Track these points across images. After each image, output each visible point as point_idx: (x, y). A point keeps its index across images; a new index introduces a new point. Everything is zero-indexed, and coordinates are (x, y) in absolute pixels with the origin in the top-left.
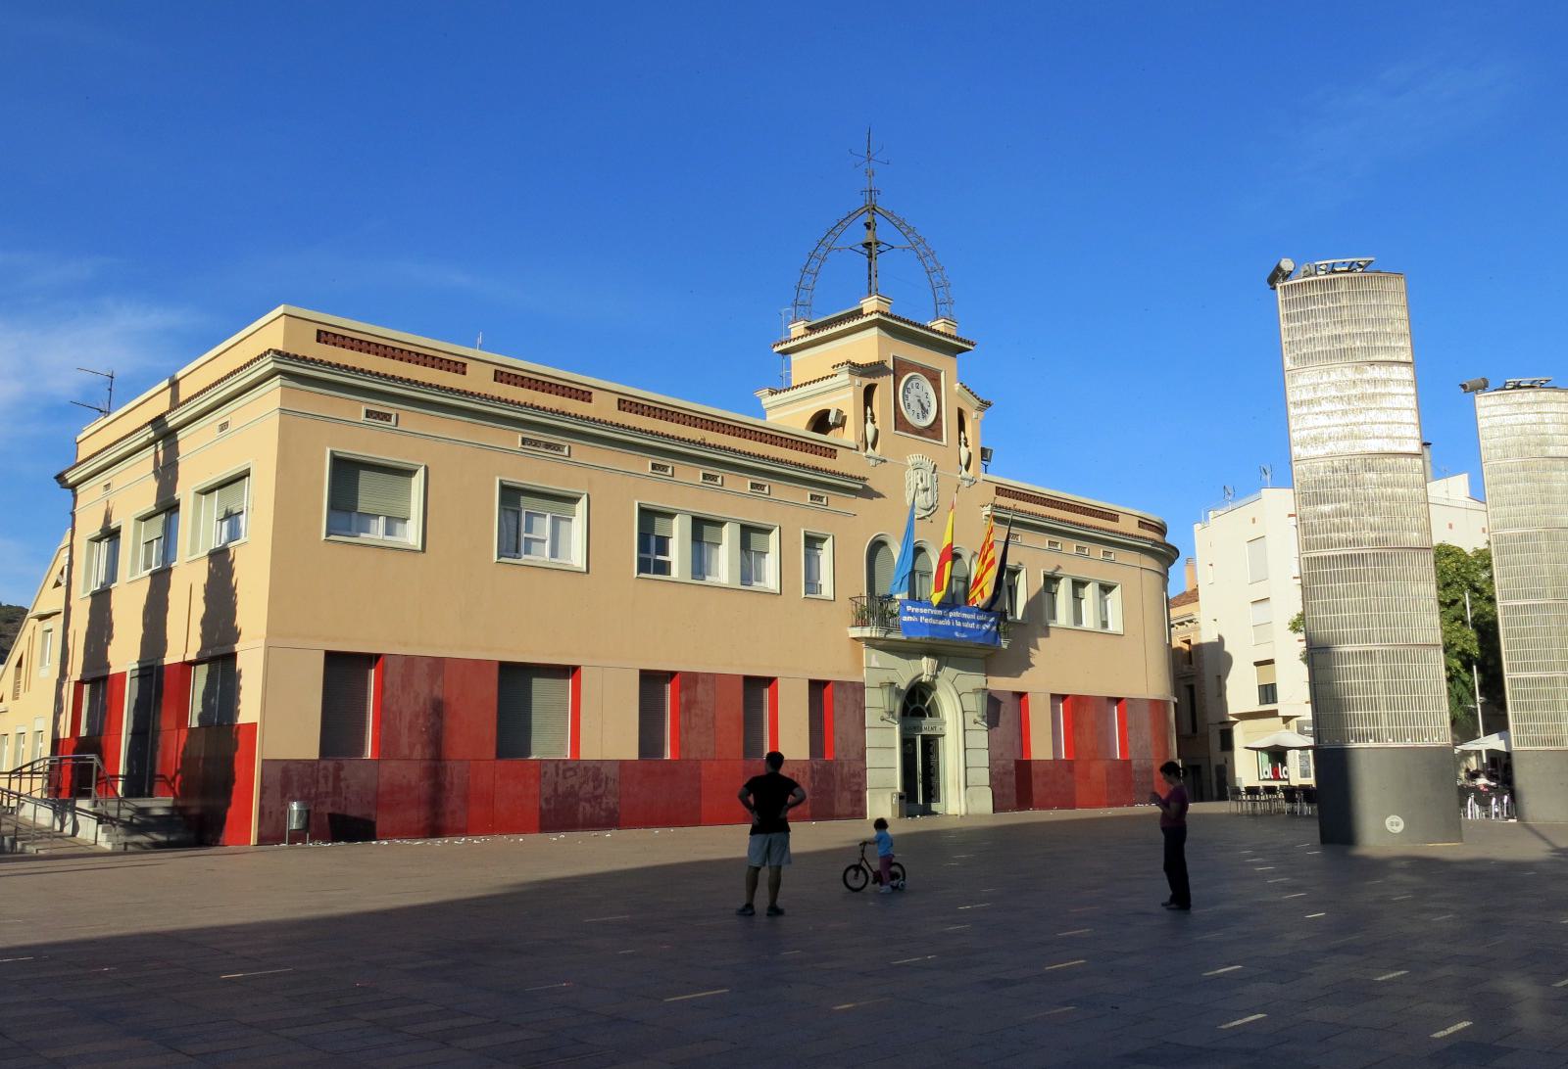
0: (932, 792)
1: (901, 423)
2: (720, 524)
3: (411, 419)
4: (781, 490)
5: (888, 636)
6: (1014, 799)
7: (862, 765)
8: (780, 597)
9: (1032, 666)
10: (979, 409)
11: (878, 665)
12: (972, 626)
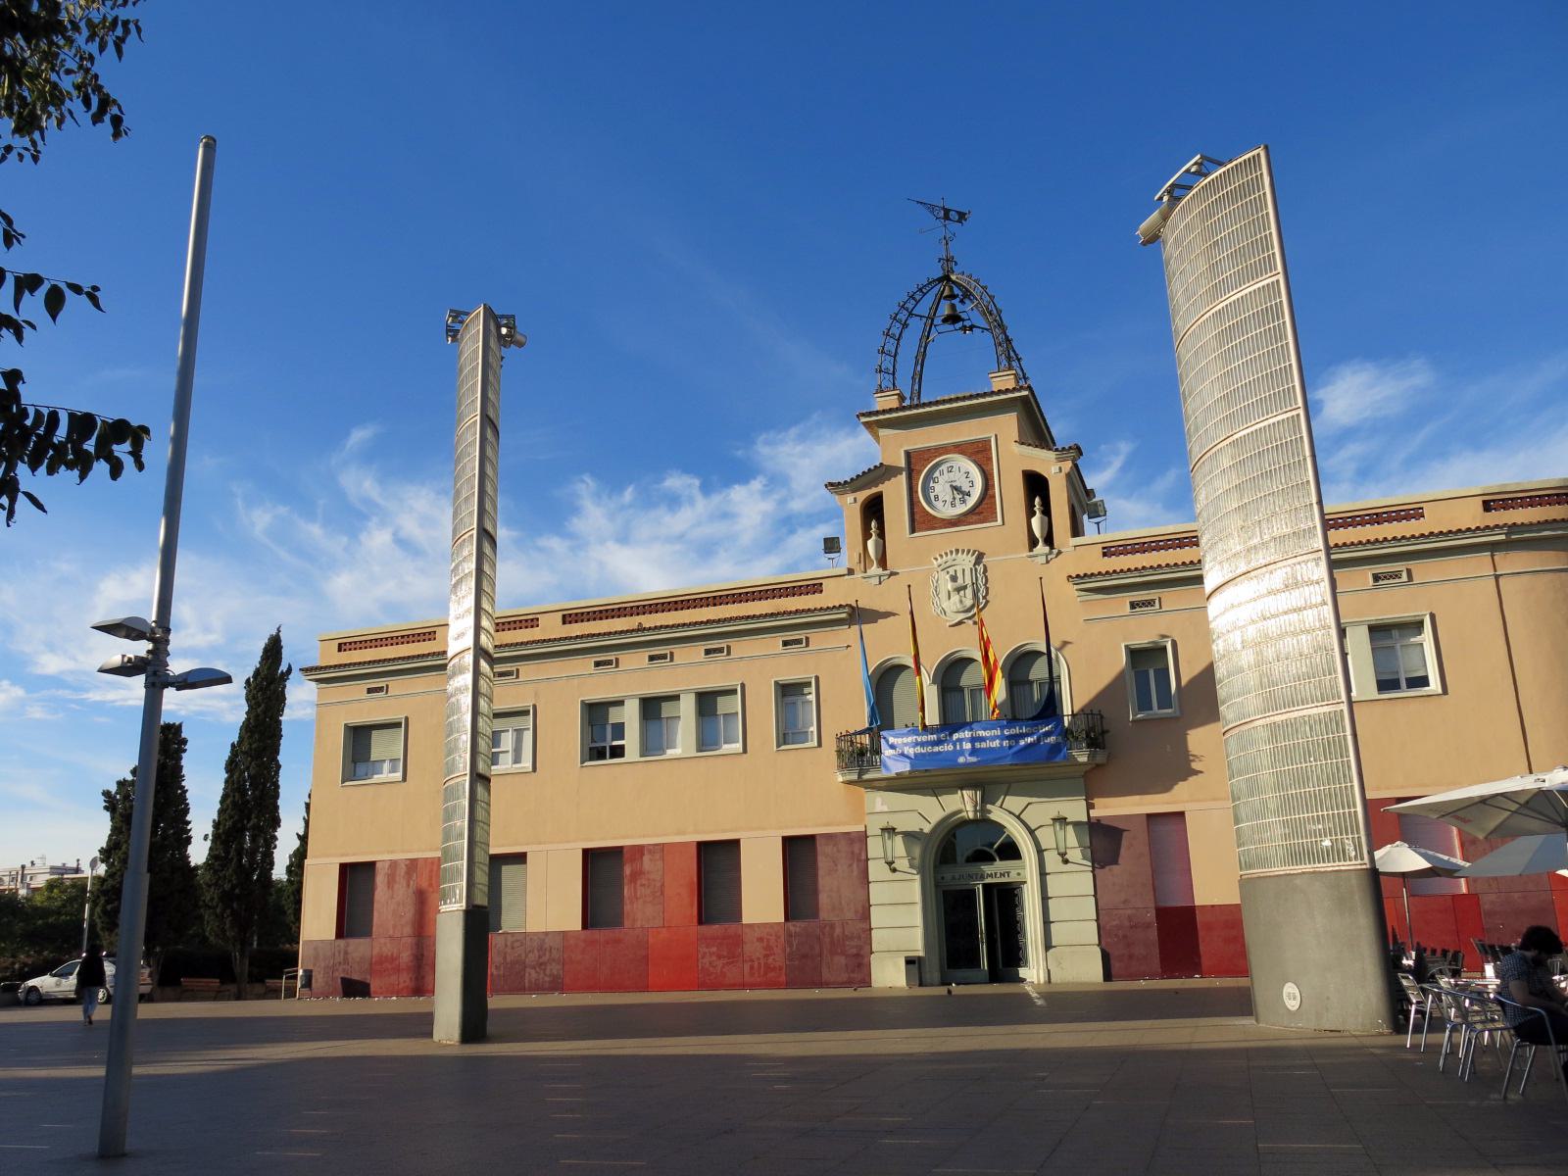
0: (1009, 955)
2: (676, 698)
3: (396, 685)
4: (741, 647)
5: (866, 777)
6: (1156, 963)
7: (863, 925)
8: (745, 755)
9: (1197, 772)
10: (1059, 460)
12: (996, 744)
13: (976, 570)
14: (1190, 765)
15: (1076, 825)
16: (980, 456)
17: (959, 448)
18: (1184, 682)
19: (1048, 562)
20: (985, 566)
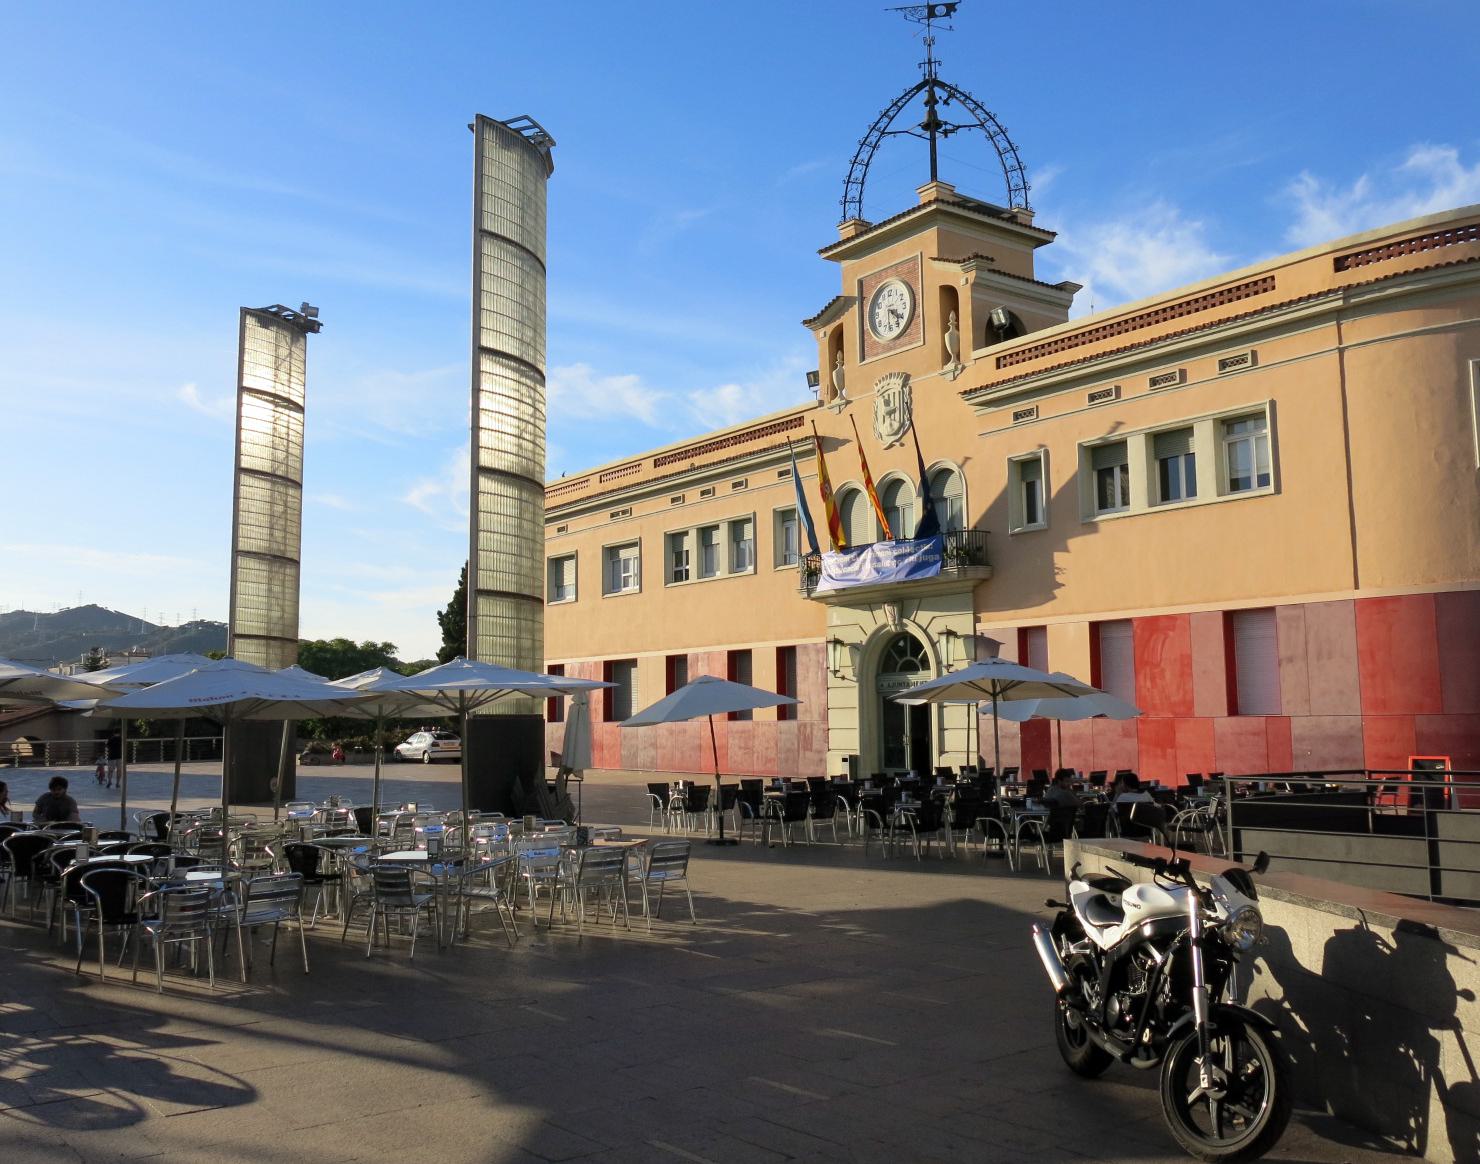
9: (1060, 585)
10: (966, 271)
11: (839, 623)
13: (903, 392)
14: (1054, 579)
15: (966, 637)
18: (1053, 493)
19: (955, 378)
20: (910, 388)
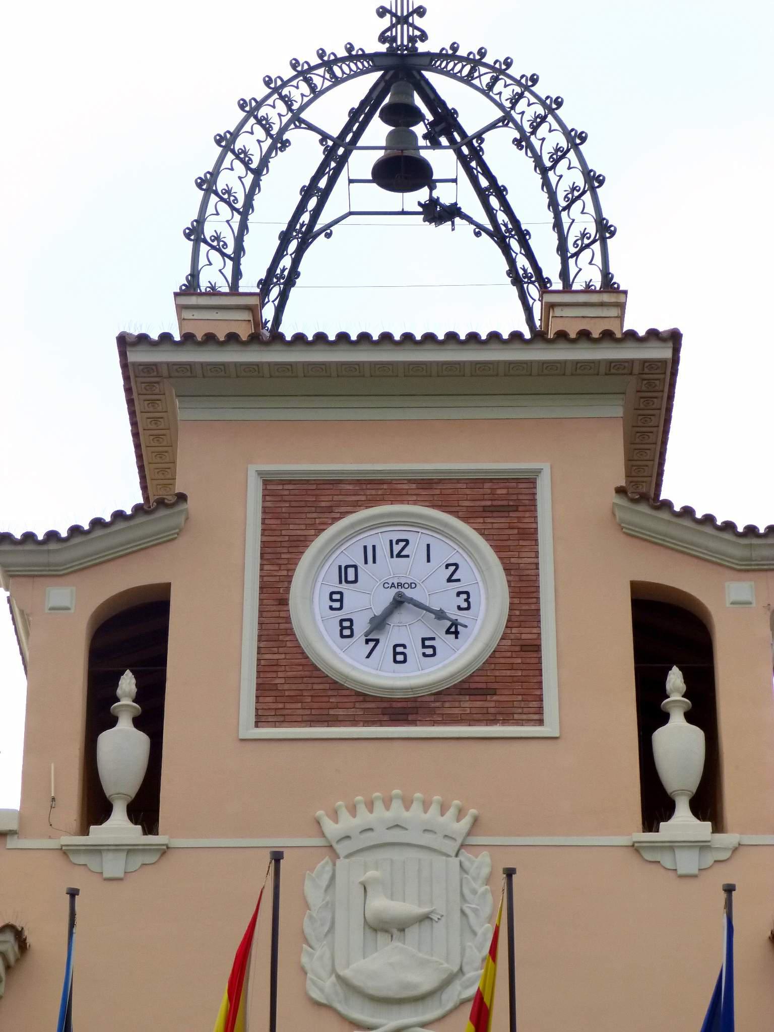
1: (295, 689)
16: (499, 522)
17: (435, 490)
